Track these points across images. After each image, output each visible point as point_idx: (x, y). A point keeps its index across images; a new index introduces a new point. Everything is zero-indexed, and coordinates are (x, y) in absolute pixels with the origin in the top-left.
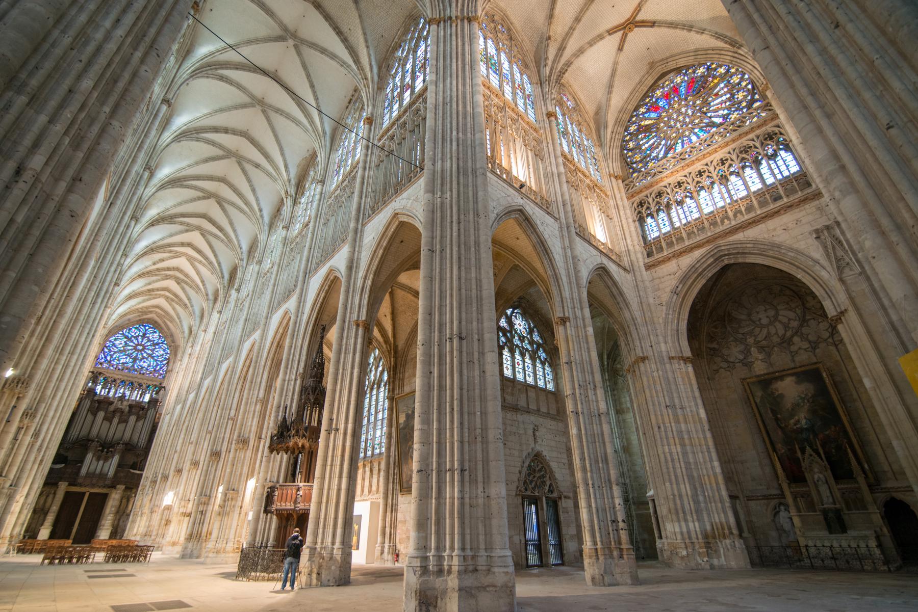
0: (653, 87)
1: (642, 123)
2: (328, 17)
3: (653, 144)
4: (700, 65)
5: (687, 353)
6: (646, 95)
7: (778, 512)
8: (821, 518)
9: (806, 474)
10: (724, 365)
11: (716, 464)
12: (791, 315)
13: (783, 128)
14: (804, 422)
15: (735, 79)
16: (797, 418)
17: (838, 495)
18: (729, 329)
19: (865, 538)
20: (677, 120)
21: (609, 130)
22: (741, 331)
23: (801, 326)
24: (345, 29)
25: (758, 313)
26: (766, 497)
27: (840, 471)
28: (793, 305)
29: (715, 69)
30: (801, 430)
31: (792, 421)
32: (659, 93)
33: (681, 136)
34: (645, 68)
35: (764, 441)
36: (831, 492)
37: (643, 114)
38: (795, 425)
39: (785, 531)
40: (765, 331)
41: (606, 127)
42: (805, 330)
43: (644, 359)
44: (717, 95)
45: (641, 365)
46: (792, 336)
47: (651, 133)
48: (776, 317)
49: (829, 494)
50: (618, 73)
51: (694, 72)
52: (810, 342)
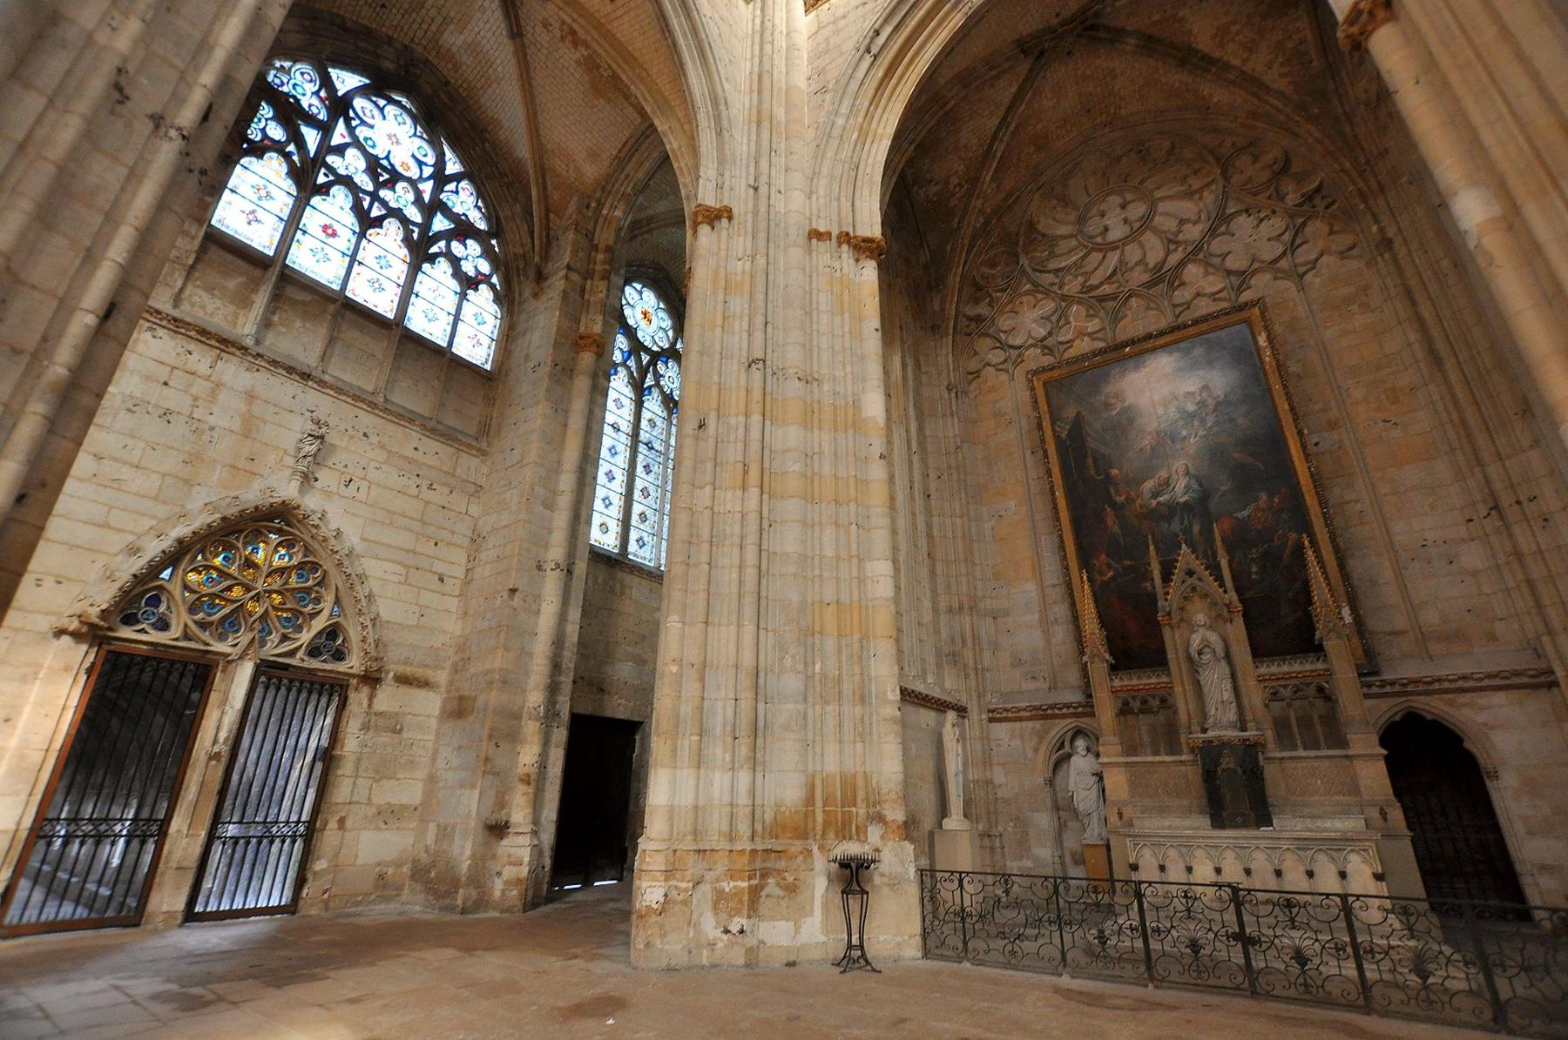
5: (871, 224)
7: (1069, 756)
8: (1194, 774)
9: (1167, 632)
10: (996, 357)
11: (881, 569)
12: (1188, 208)
14: (1181, 484)
16: (1164, 474)
17: (1255, 697)
18: (1024, 261)
19: (1336, 845)
22: (1053, 265)
23: (1212, 232)
25: (1103, 215)
26: (1043, 713)
27: (1280, 623)
28: (1196, 184)
30: (1172, 509)
31: (1149, 485)
35: (1062, 547)
36: (1236, 689)
38: (1155, 496)
39: (1075, 812)
40: (1113, 259)
42: (1217, 246)
43: (715, 216)
45: (704, 229)
46: (1182, 264)
48: (1146, 222)
49: (1228, 695)
52: (1229, 272)
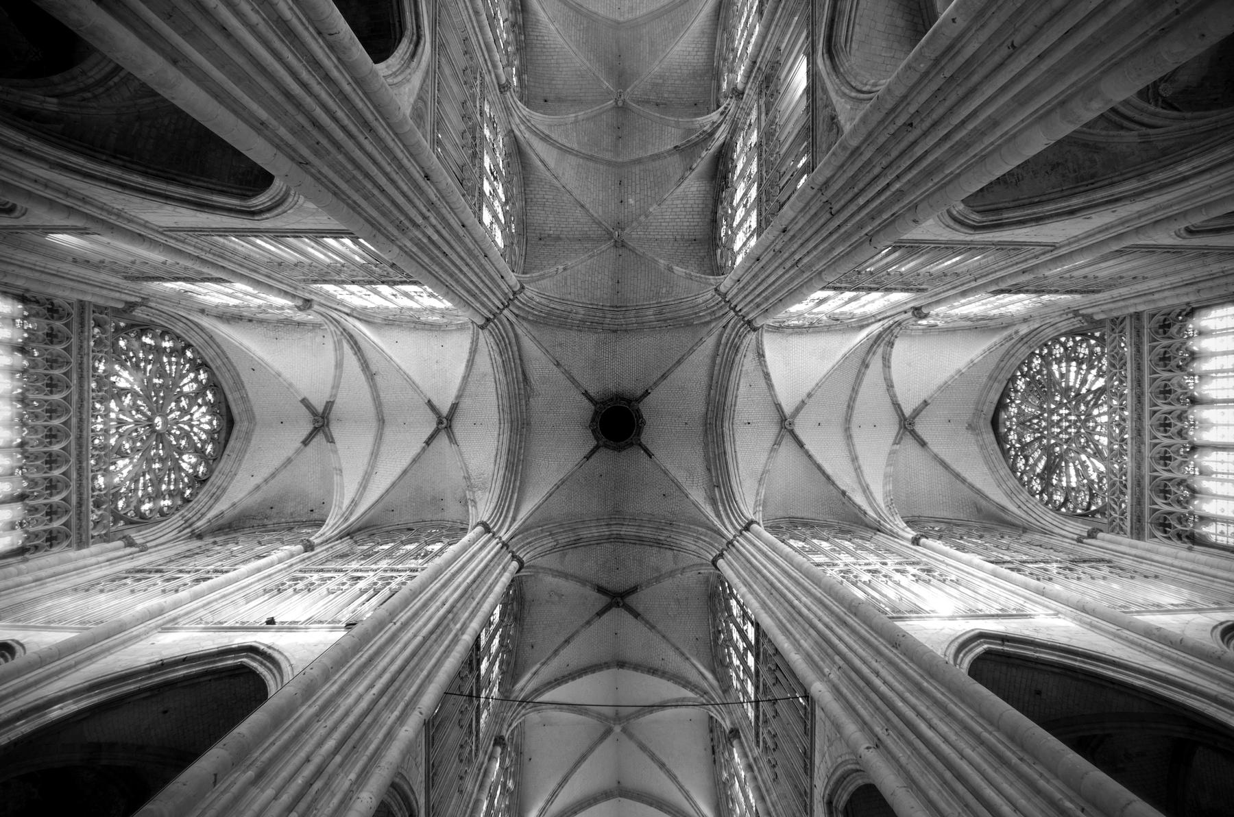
0: (1001, 439)
1: (1038, 470)
2: (636, 667)
3: (1077, 471)
4: (1013, 379)
6: (1005, 453)
13: (1160, 309)
15: (1058, 351)
20: (1065, 431)
21: (1012, 508)
24: (657, 663)
29: (1030, 369)
32: (1013, 436)
33: (1090, 433)
34: (969, 434)
37: (1026, 465)
41: (1003, 509)
44: (1062, 375)
47: (1058, 466)
50: (948, 460)
51: (1016, 391)
